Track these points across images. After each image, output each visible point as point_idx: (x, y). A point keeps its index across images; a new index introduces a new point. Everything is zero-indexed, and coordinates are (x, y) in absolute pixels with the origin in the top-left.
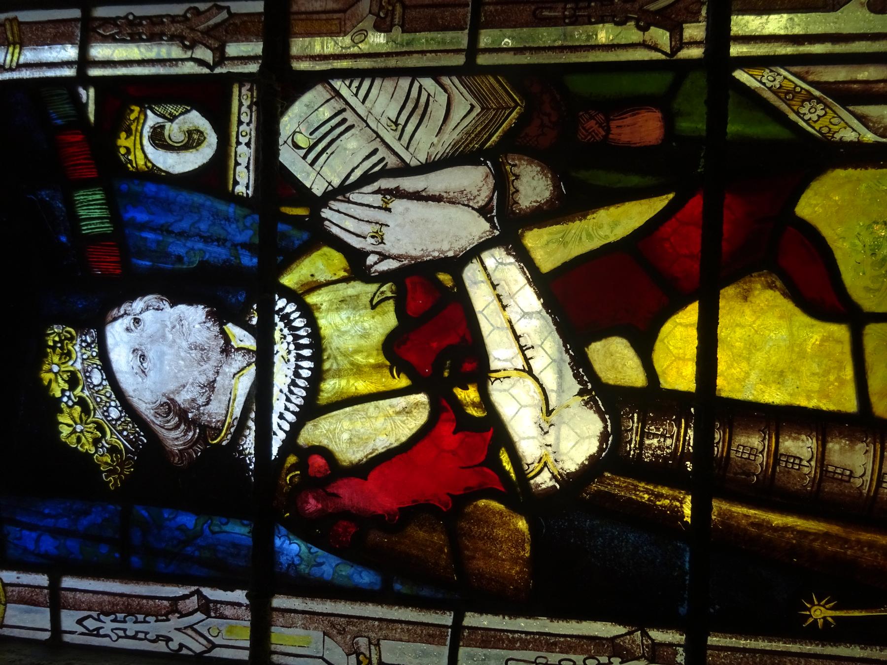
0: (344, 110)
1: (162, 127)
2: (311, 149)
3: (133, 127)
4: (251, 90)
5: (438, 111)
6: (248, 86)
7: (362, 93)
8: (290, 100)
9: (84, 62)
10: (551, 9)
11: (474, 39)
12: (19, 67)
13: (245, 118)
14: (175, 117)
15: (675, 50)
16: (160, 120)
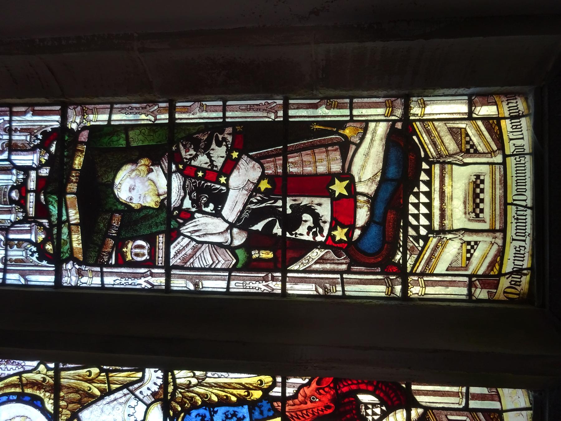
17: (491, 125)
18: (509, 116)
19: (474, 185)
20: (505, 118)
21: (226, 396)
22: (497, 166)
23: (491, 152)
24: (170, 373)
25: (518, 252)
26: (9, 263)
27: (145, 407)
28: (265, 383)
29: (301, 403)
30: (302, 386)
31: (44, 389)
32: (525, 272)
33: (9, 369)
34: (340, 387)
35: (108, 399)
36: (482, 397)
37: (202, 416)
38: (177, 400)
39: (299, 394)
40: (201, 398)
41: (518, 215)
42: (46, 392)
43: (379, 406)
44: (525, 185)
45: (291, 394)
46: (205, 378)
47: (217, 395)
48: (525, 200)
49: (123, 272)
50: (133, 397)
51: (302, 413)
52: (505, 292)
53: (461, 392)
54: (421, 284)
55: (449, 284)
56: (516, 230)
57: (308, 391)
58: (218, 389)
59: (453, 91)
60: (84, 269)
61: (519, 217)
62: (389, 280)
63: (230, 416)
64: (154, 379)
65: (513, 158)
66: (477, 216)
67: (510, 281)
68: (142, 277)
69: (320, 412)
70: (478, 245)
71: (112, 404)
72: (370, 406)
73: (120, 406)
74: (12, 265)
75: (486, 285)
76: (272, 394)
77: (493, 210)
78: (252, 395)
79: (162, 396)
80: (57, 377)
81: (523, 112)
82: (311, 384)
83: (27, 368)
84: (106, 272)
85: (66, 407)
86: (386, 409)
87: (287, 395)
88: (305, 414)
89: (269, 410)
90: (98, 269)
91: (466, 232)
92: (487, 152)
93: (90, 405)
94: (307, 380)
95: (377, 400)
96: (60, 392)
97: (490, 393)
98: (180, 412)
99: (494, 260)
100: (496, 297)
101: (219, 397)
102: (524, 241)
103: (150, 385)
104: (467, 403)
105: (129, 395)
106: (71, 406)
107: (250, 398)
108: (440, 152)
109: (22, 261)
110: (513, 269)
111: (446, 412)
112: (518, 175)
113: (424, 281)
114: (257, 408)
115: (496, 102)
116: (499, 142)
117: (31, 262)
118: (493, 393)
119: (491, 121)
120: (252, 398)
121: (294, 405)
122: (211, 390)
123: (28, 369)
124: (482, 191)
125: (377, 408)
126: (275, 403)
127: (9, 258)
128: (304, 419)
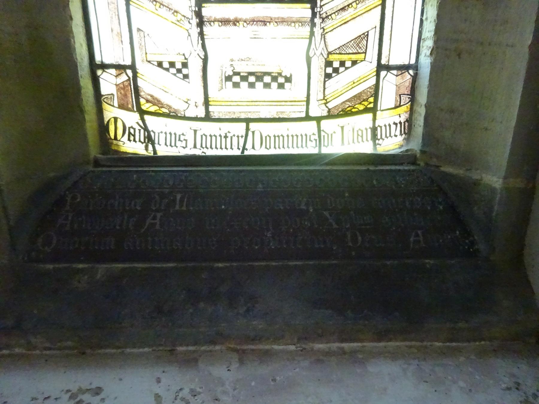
17: (366, 100)
18: (376, 126)
19: (275, 73)
20: (374, 119)
22: (304, 108)
23: (326, 100)
25: (178, 138)
32: (150, 147)
41: (231, 137)
44: (275, 147)
48: (253, 148)
52: (116, 119)
56: (211, 136)
59: (430, 28)
61: (229, 140)
65: (316, 131)
66: (228, 78)
67: (134, 127)
70: (183, 79)
75: (122, 91)
77: (238, 103)
81: (380, 145)
91: (203, 62)
92: (326, 93)
99: (162, 104)
100: (105, 106)
102: (195, 147)
108: (330, 17)
110: (152, 131)
112: (290, 138)
115: (400, 106)
116: (340, 112)
119: (372, 99)
124: (267, 86)
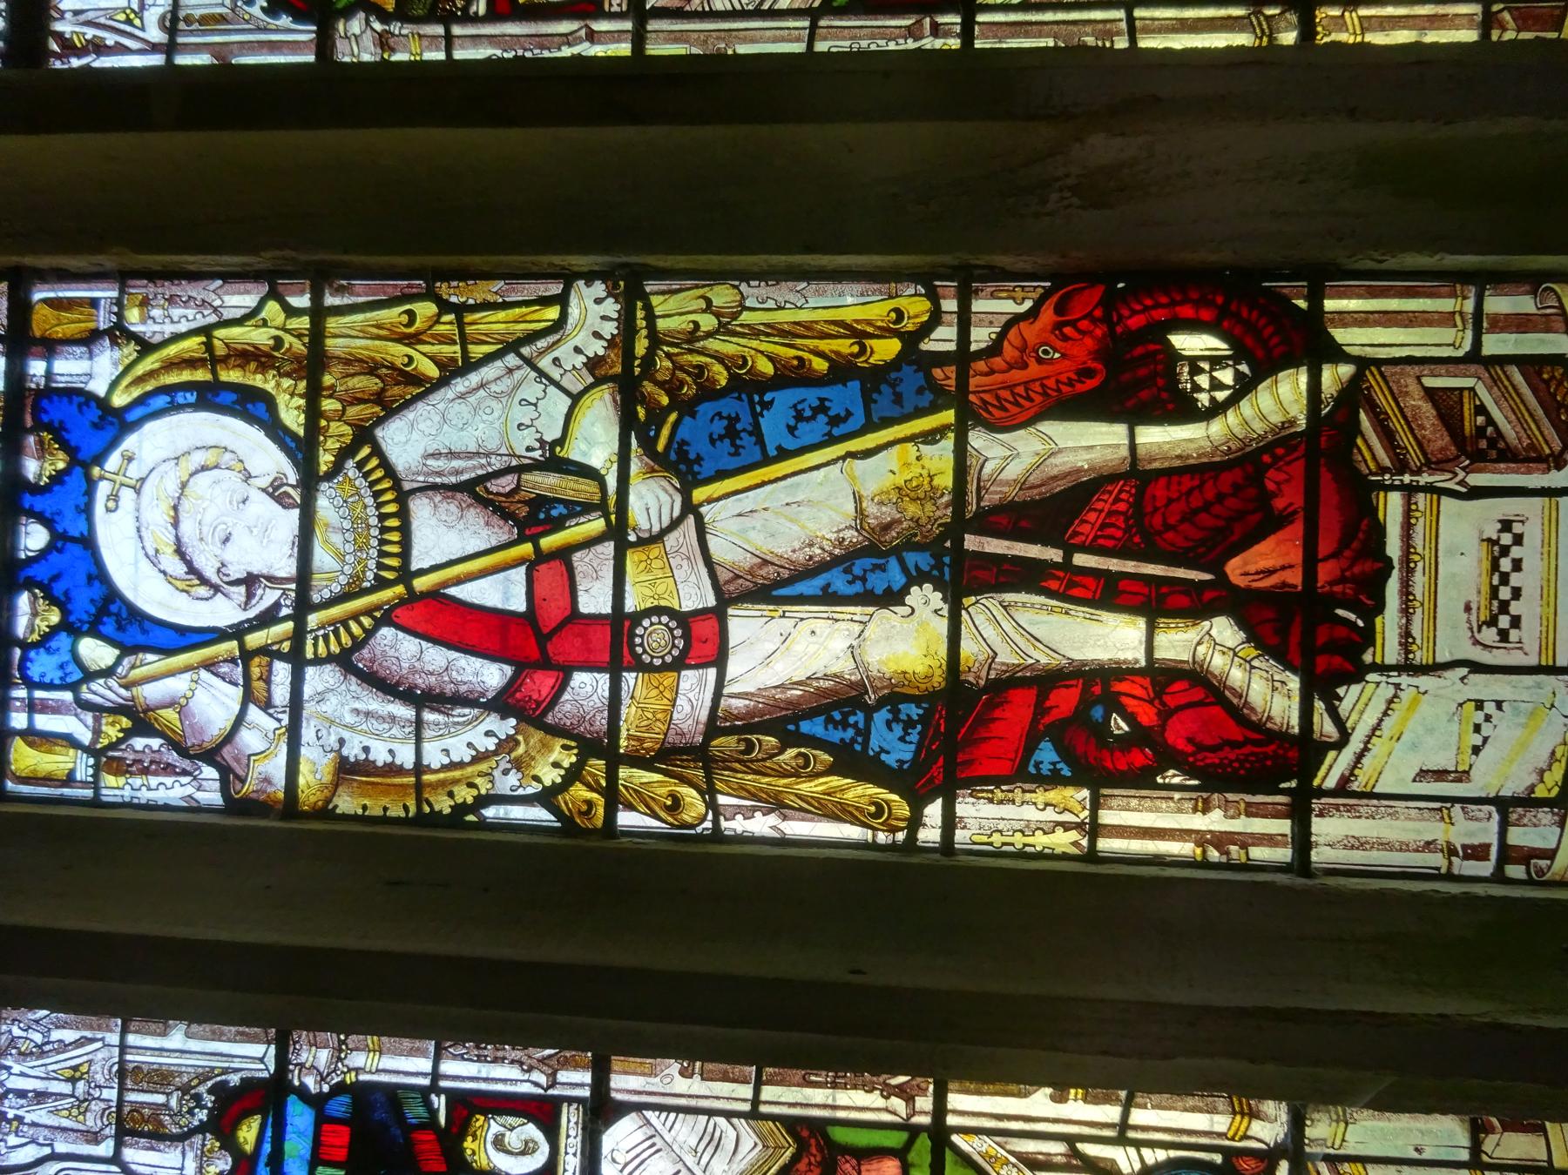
0: (653, 1136)
1: (503, 1135)
2: (626, 1165)
3: (478, 1133)
4: (578, 1109)
5: (729, 1143)
6: (575, 1106)
7: (669, 1124)
8: (609, 1123)
9: (436, 1075)
10: (816, 1075)
11: (757, 1092)
12: (378, 1071)
13: (573, 1133)
14: (514, 1128)
15: (909, 1118)
16: (502, 1129)
21: (800, 359)
24: (639, 304)
26: (182, 26)
27: (568, 401)
28: (909, 318)
29: (1011, 367)
30: (1016, 319)
31: (278, 369)
33: (176, 319)
34: (1120, 317)
35: (460, 385)
36: (1520, 323)
37: (729, 418)
38: (660, 377)
39: (1006, 343)
40: (727, 368)
42: (281, 375)
43: (1231, 363)
45: (983, 345)
46: (740, 313)
47: (772, 358)
49: (510, 36)
50: (533, 374)
51: (1013, 394)
53: (1461, 313)
54: (1350, 27)
55: (1427, 24)
57: (1030, 331)
58: (776, 339)
60: (397, 32)
62: (1262, 18)
63: (808, 413)
64: (594, 322)
68: (564, 44)
69: (1064, 388)
71: (472, 399)
72: (1206, 366)
73: (494, 404)
74: (191, 31)
76: (927, 346)
78: (872, 352)
79: (618, 369)
80: (317, 335)
82: (1039, 312)
83: (228, 314)
84: (458, 37)
85: (340, 416)
86: (1251, 369)
87: (974, 347)
88: (1021, 396)
89: (920, 391)
90: (439, 30)
93: (407, 404)
94: (1028, 304)
95: (1225, 346)
96: (323, 375)
97: (1540, 312)
98: (667, 411)
101: (779, 362)
103: (581, 338)
104: (1477, 343)
105: (522, 372)
106: (353, 411)
107: (866, 361)
109: (222, 19)
111: (1417, 369)
113: (1360, 18)
114: (884, 388)
117: (247, 22)
118: (1549, 311)
120: (871, 361)
121: (992, 372)
122: (754, 344)
123: (230, 317)
125: (1224, 368)
126: (939, 370)
127: (182, 14)
128: (1018, 410)
